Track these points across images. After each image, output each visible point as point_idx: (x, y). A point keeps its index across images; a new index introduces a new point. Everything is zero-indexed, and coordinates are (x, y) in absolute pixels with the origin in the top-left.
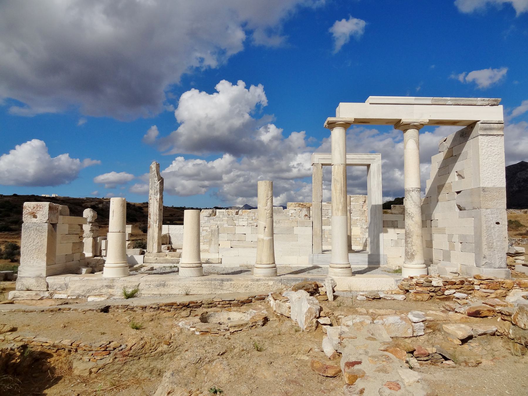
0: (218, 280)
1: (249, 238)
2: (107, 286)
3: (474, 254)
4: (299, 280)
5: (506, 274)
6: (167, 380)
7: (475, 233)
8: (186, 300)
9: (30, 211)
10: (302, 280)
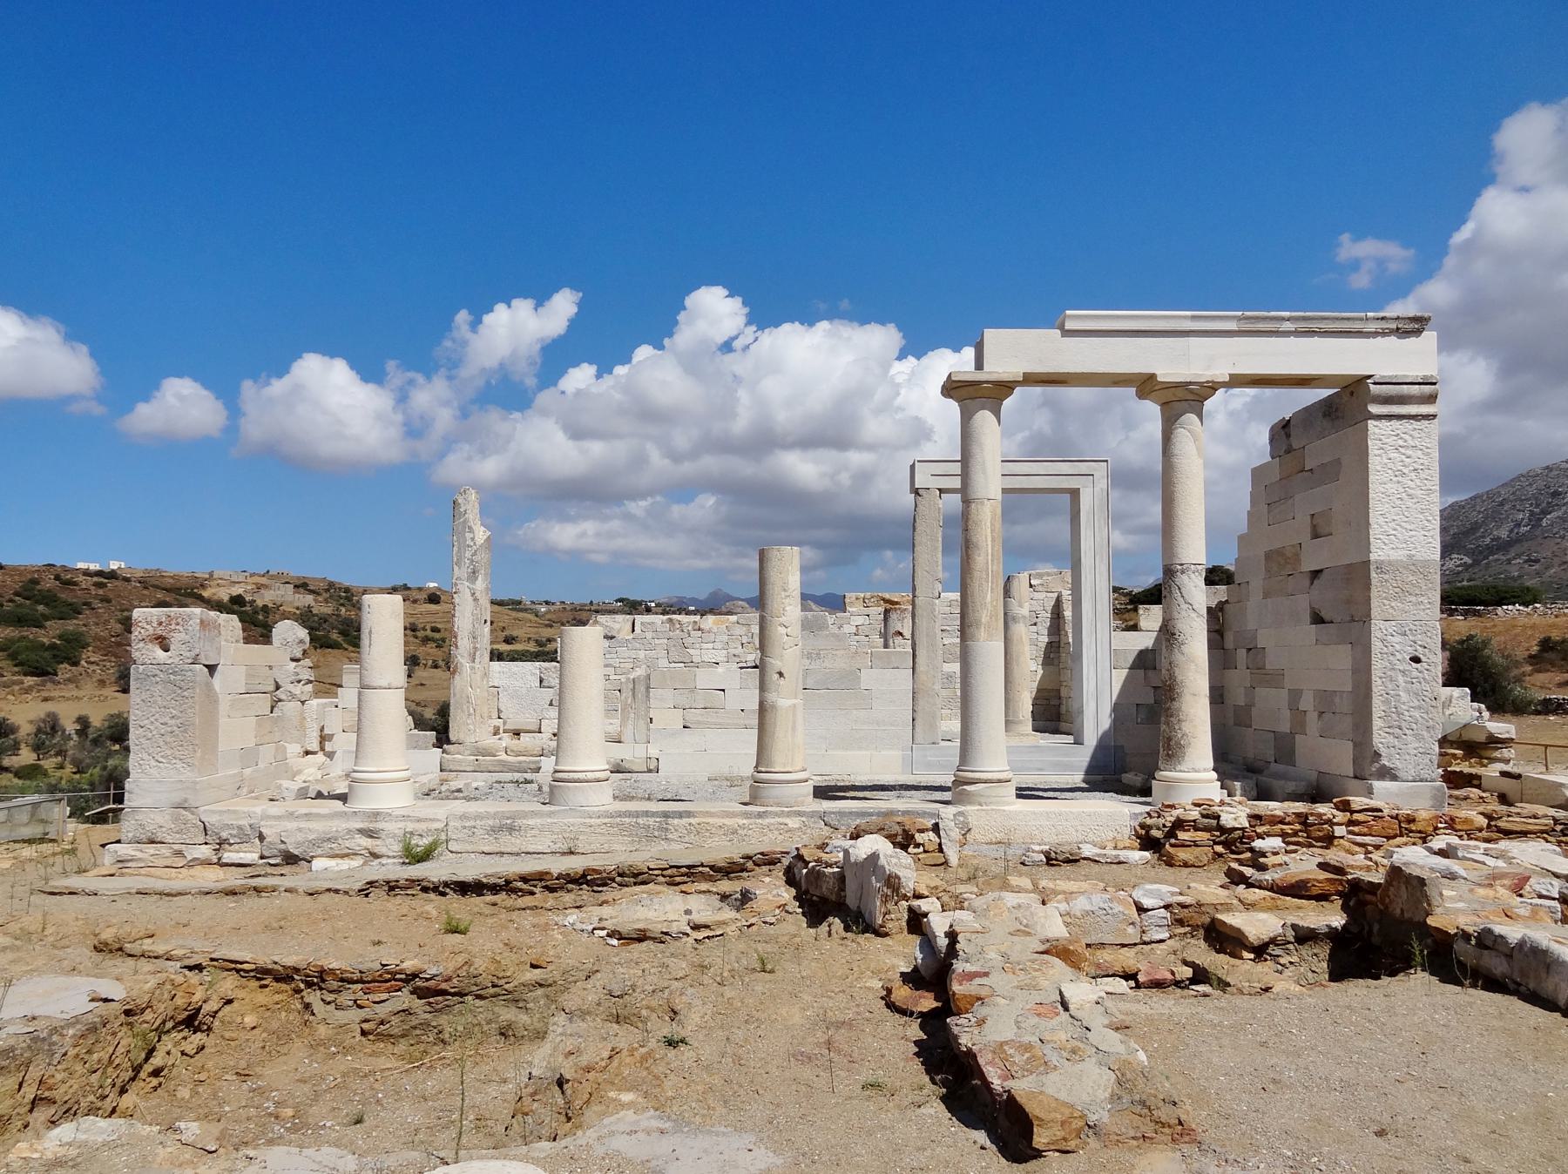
0: (654, 814)
2: (361, 831)
4: (871, 814)
5: (1435, 797)
6: (560, 1030)
7: (1356, 686)
8: (575, 864)
10: (879, 814)
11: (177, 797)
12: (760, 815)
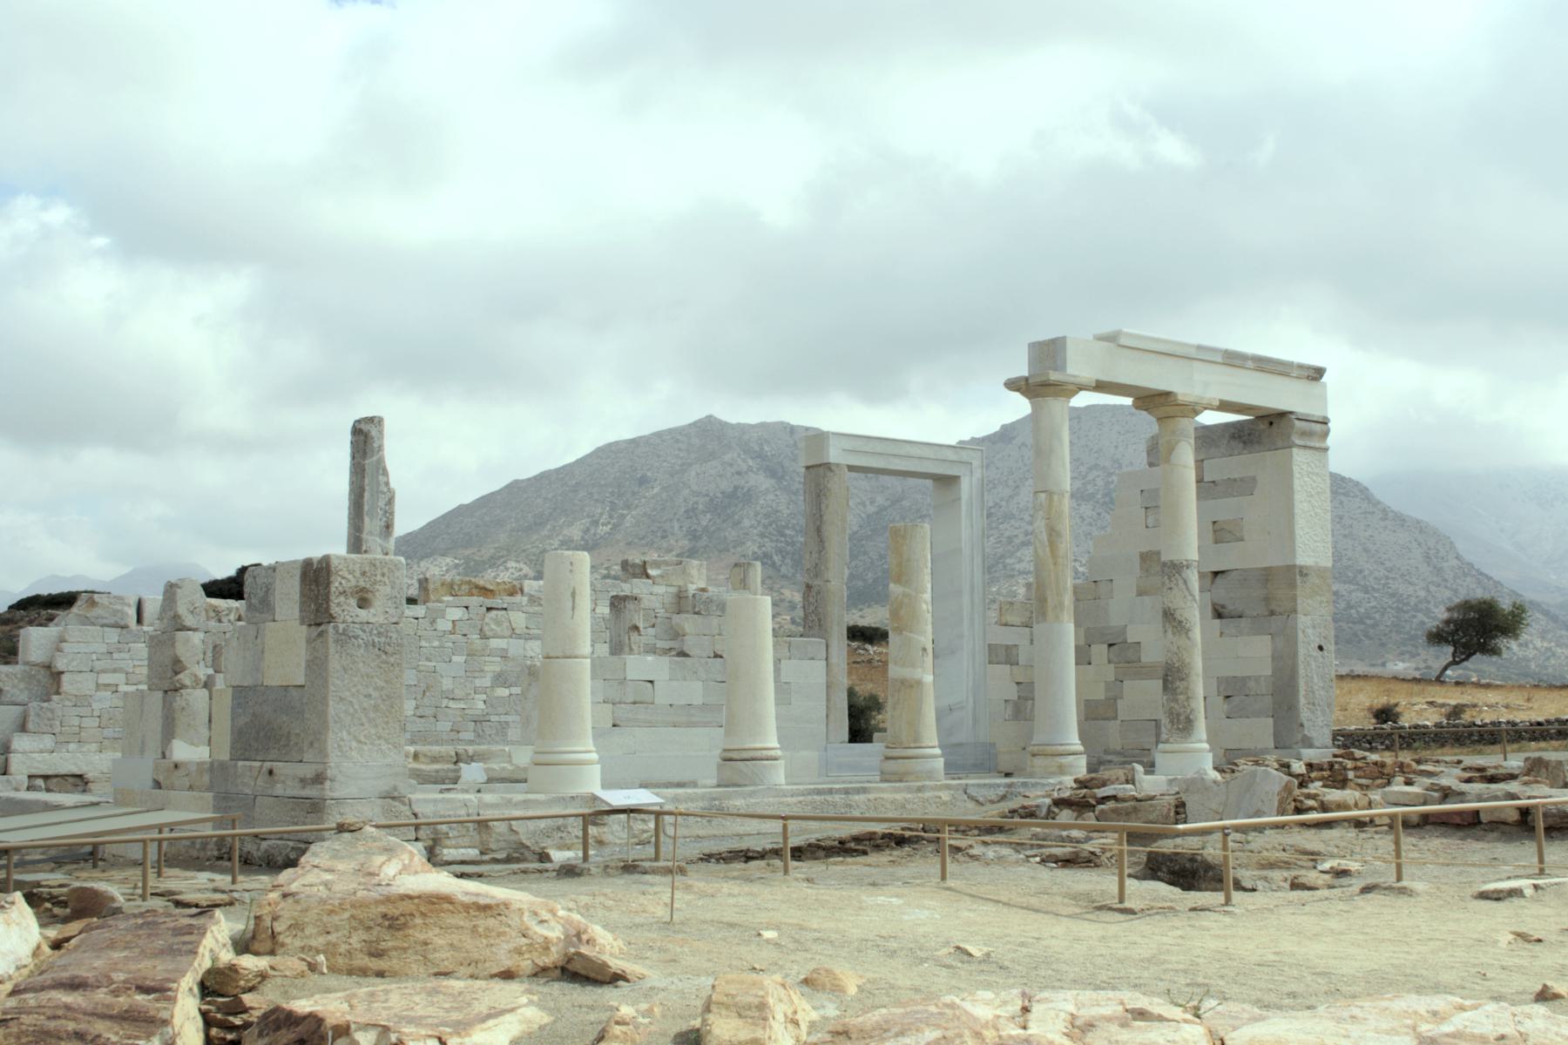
0: (838, 791)
1: (662, 695)
3: (1270, 721)
9: (353, 583)
11: (384, 785)
12: (920, 789)
